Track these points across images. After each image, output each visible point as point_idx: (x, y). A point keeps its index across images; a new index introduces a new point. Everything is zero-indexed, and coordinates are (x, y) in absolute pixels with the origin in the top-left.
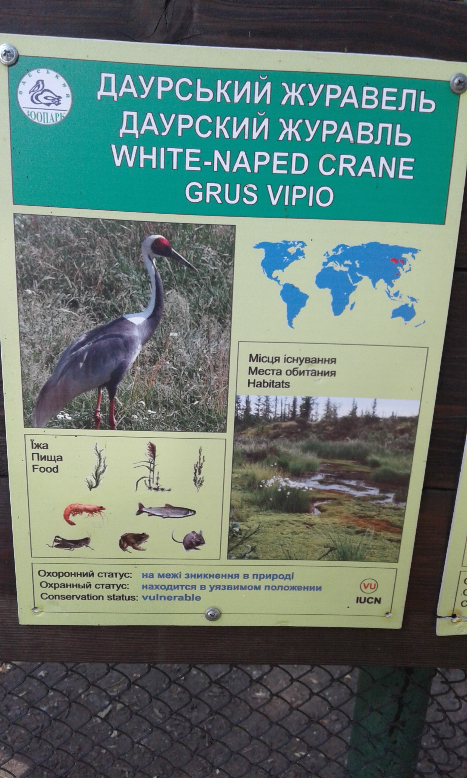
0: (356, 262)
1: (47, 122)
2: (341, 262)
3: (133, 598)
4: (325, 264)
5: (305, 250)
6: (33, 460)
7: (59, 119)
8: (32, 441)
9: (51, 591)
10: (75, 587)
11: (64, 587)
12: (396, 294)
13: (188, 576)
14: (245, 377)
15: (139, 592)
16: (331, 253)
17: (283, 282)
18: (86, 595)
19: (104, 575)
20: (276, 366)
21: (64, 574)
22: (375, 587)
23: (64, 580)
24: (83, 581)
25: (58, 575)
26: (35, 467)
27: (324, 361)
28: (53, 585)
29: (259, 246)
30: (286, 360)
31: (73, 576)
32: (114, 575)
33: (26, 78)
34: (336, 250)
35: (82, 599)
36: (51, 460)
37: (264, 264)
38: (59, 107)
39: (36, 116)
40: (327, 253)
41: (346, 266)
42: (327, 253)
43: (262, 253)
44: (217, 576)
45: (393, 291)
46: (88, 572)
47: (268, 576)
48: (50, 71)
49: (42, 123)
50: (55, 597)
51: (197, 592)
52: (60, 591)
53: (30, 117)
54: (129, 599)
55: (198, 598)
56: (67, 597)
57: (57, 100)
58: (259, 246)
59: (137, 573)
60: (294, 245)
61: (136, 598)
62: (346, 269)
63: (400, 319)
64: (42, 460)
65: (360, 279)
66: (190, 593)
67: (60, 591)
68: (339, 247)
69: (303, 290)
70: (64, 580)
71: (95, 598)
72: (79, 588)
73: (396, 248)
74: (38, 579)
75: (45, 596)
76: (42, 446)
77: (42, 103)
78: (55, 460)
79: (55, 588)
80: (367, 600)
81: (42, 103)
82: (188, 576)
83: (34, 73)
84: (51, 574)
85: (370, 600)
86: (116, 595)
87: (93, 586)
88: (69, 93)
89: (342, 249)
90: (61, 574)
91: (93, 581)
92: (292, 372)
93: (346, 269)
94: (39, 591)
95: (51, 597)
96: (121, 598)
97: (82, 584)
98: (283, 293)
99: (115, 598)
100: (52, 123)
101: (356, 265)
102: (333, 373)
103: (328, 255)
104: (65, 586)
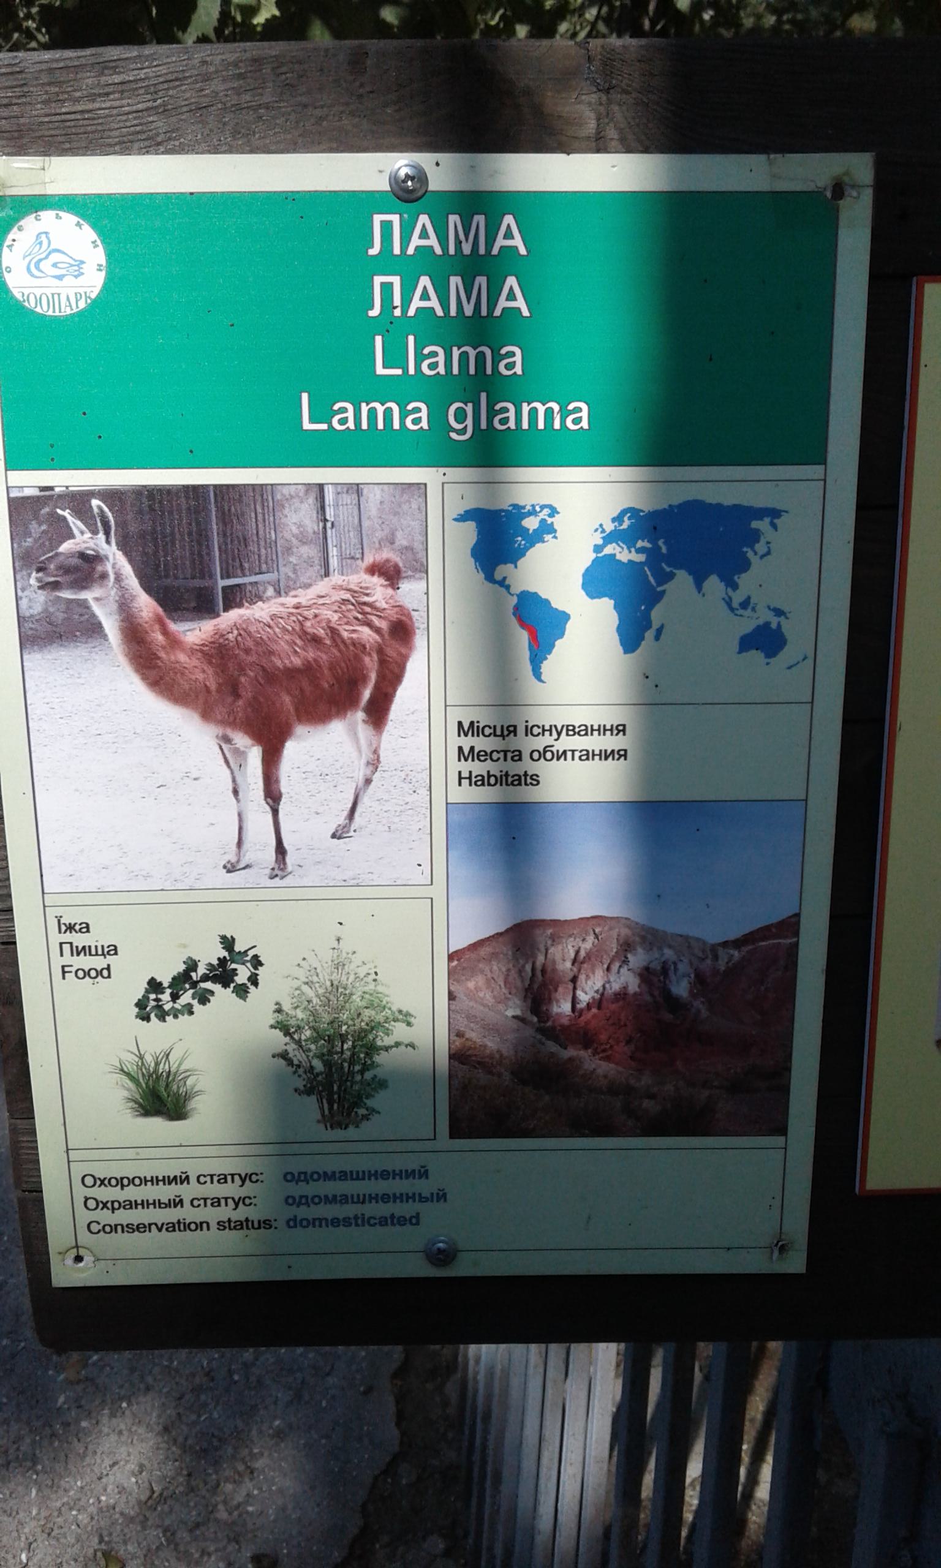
0: (661, 543)
1: (60, 312)
4: (598, 549)
6: (62, 955)
7: (82, 305)
9: (106, 1217)
10: (151, 1207)
11: (131, 1208)
16: (609, 527)
18: (175, 1221)
19: (208, 1179)
24: (165, 1192)
25: (121, 1182)
26: (67, 969)
28: (109, 1205)
31: (149, 1184)
32: (229, 1178)
34: (618, 519)
35: (167, 1229)
36: (97, 954)
38: (81, 280)
39: (39, 301)
40: (601, 525)
41: (638, 551)
42: (601, 525)
46: (178, 1174)
48: (61, 213)
49: (50, 313)
50: (114, 1228)
52: (123, 1217)
53: (26, 304)
54: (259, 1228)
56: (140, 1228)
61: (274, 1224)
64: (78, 954)
67: (123, 1217)
70: (132, 1193)
71: (193, 1226)
72: (160, 1207)
74: (80, 1192)
75: (95, 1227)
76: (77, 927)
77: (48, 276)
78: (103, 954)
79: (113, 1209)
81: (48, 276)
84: (106, 1182)
86: (233, 1219)
87: (187, 1203)
89: (629, 518)
90: (125, 1182)
91: (187, 1192)
95: (108, 1229)
97: (165, 1200)
99: (233, 1225)
100: (69, 312)
101: (660, 548)
103: (603, 531)
104: (131, 1205)
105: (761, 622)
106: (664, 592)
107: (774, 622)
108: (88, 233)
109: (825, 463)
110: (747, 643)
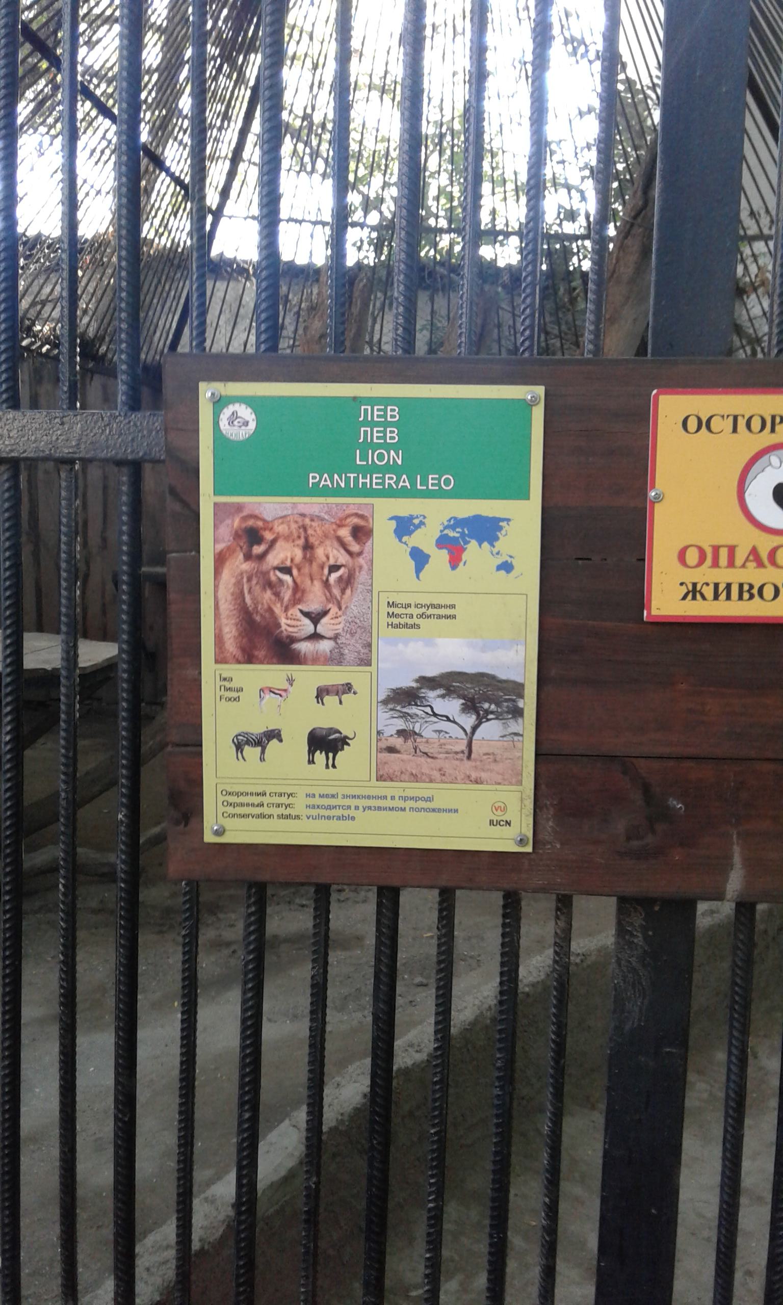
2: (454, 530)
4: (441, 531)
5: (426, 521)
12: (498, 553)
13: (344, 797)
14: (384, 620)
16: (446, 523)
17: (411, 545)
20: (409, 611)
21: (242, 794)
22: (505, 809)
24: (257, 800)
25: (238, 794)
27: (446, 607)
29: (391, 519)
30: (416, 606)
34: (449, 520)
37: (396, 531)
43: (393, 524)
44: (369, 797)
45: (495, 551)
47: (412, 798)
50: (234, 816)
51: (352, 812)
52: (239, 810)
55: (353, 818)
58: (391, 519)
59: (301, 792)
60: (417, 517)
62: (458, 535)
63: (503, 572)
65: (469, 542)
66: (346, 813)
67: (239, 810)
69: (426, 551)
74: (221, 798)
82: (344, 797)
87: (265, 805)
91: (266, 800)
92: (421, 616)
97: (256, 803)
98: (411, 554)
102: (454, 617)
104: (242, 805)
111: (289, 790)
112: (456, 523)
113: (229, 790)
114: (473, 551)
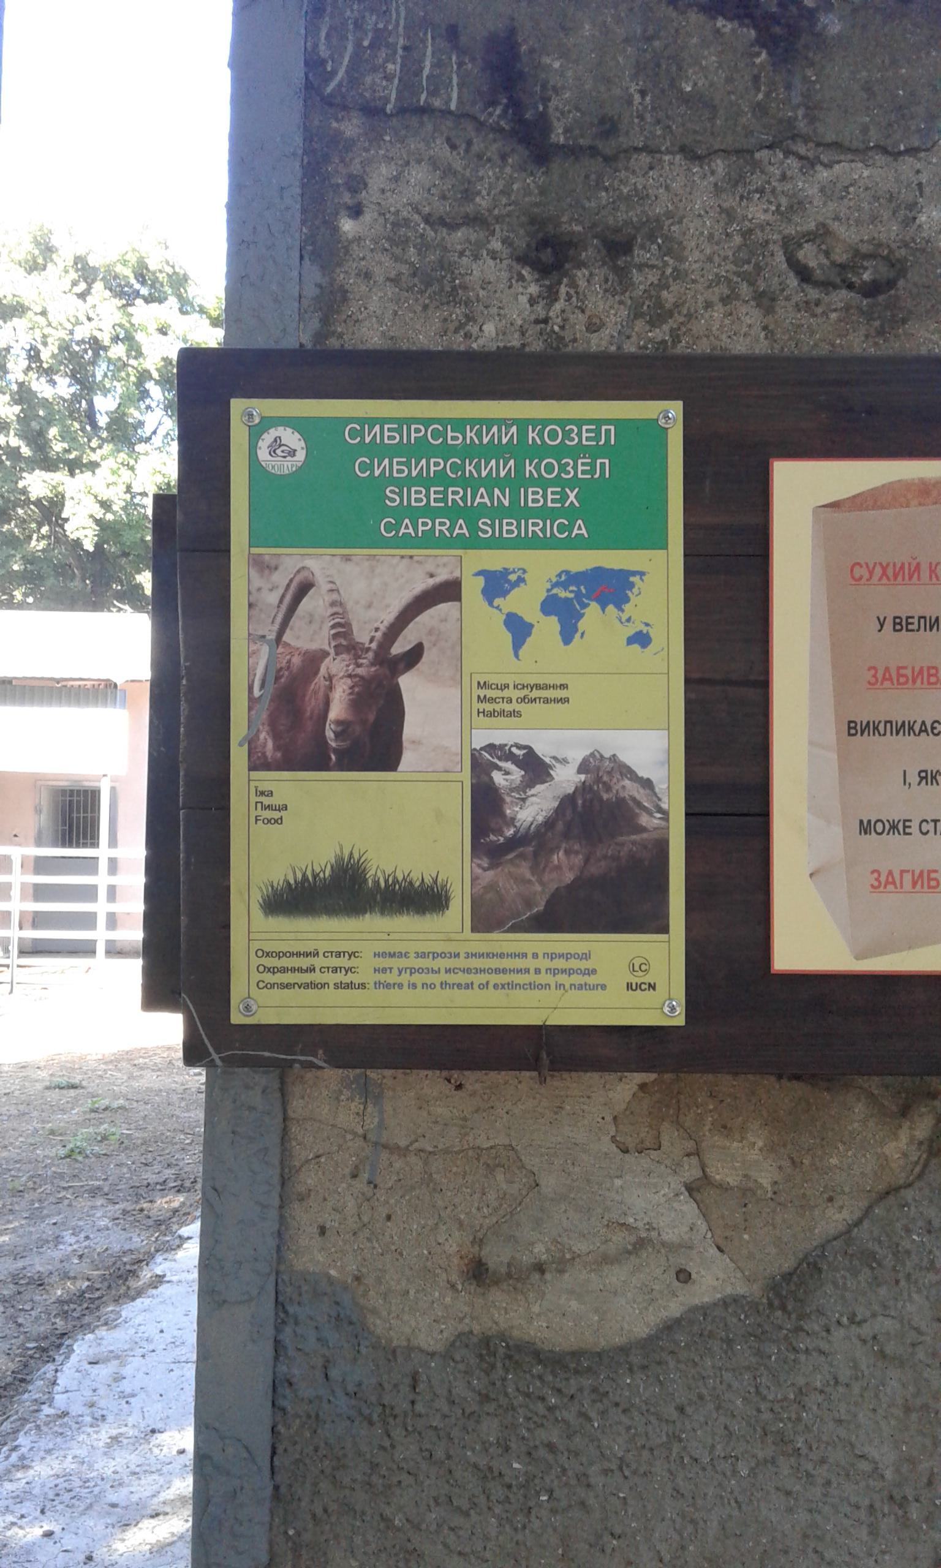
0: (582, 588)
3: (363, 986)
4: (548, 591)
8: (256, 788)
15: (370, 978)
16: (554, 580)
23: (286, 962)
25: (279, 955)
33: (265, 436)
34: (559, 575)
38: (295, 459)
39: (273, 467)
50: (272, 986)
52: (279, 978)
56: (287, 986)
57: (293, 453)
59: (367, 949)
62: (572, 595)
67: (279, 978)
68: (562, 572)
70: (286, 962)
73: (621, 571)
74: (255, 961)
79: (274, 973)
80: (639, 986)
83: (272, 431)
85: (643, 987)
88: (303, 445)
91: (318, 962)
93: (572, 595)
94: (256, 977)
96: (350, 986)
100: (286, 472)
104: (284, 970)
105: (638, 630)
106: (584, 614)
107: (645, 630)
108: (297, 435)
109: (667, 548)
110: (630, 641)
111: (349, 947)
112: (569, 579)
113: (267, 949)
114: (592, 615)
